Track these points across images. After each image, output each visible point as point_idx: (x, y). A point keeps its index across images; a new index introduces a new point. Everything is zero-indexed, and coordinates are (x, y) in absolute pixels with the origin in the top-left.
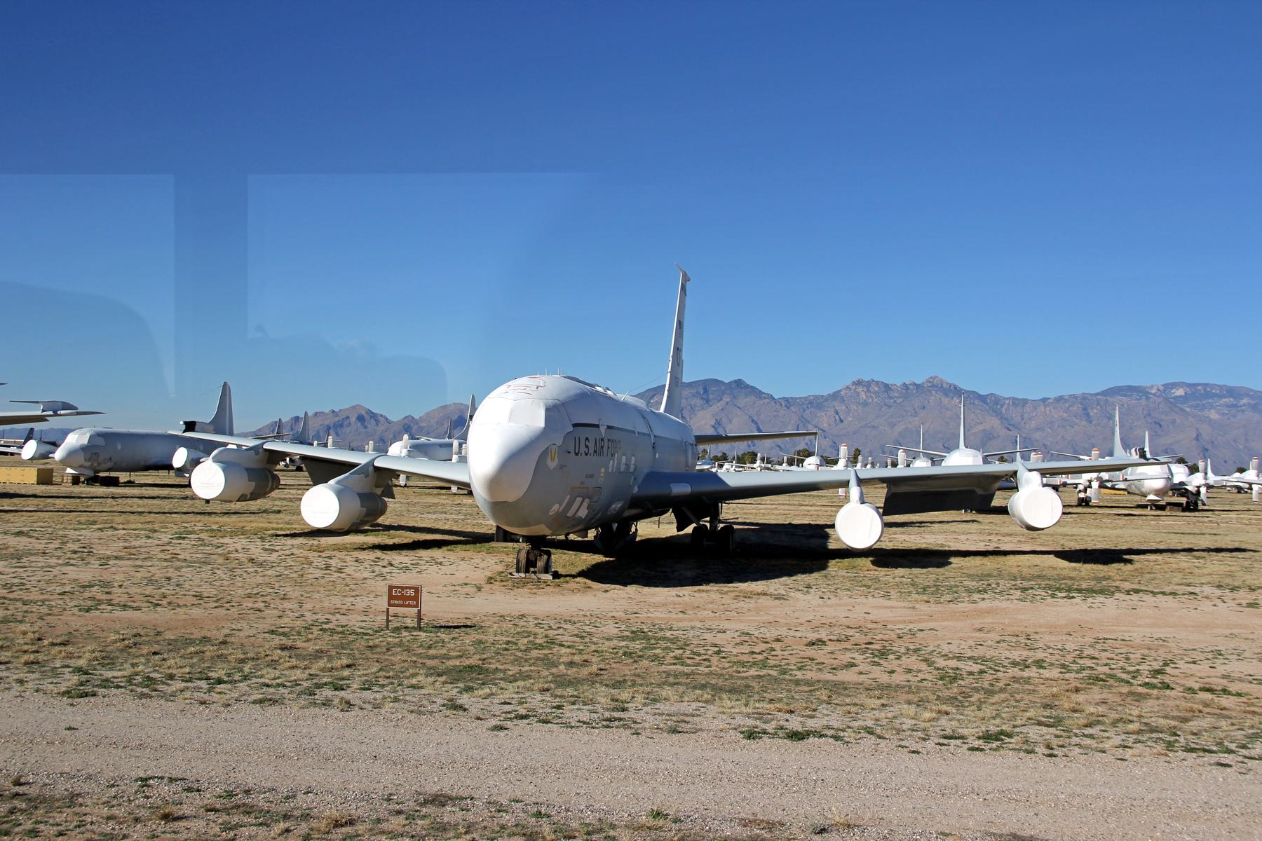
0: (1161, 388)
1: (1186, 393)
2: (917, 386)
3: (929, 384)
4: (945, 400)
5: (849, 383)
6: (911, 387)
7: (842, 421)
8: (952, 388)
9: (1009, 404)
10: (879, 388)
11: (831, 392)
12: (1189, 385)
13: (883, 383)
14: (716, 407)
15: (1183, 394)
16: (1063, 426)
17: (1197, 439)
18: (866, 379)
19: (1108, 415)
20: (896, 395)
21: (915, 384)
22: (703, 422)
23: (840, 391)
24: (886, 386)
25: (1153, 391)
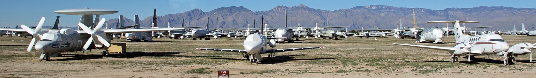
0: (369, 7)
3: (300, 7)
4: (304, 11)
5: (275, 7)
6: (295, 8)
7: (273, 18)
11: (270, 10)
12: (377, 6)
14: (234, 15)
15: (375, 8)
16: (339, 19)
17: (376, 22)
18: (281, 5)
19: (352, 15)
21: (296, 7)
22: (229, 20)
23: (273, 9)
24: (287, 7)
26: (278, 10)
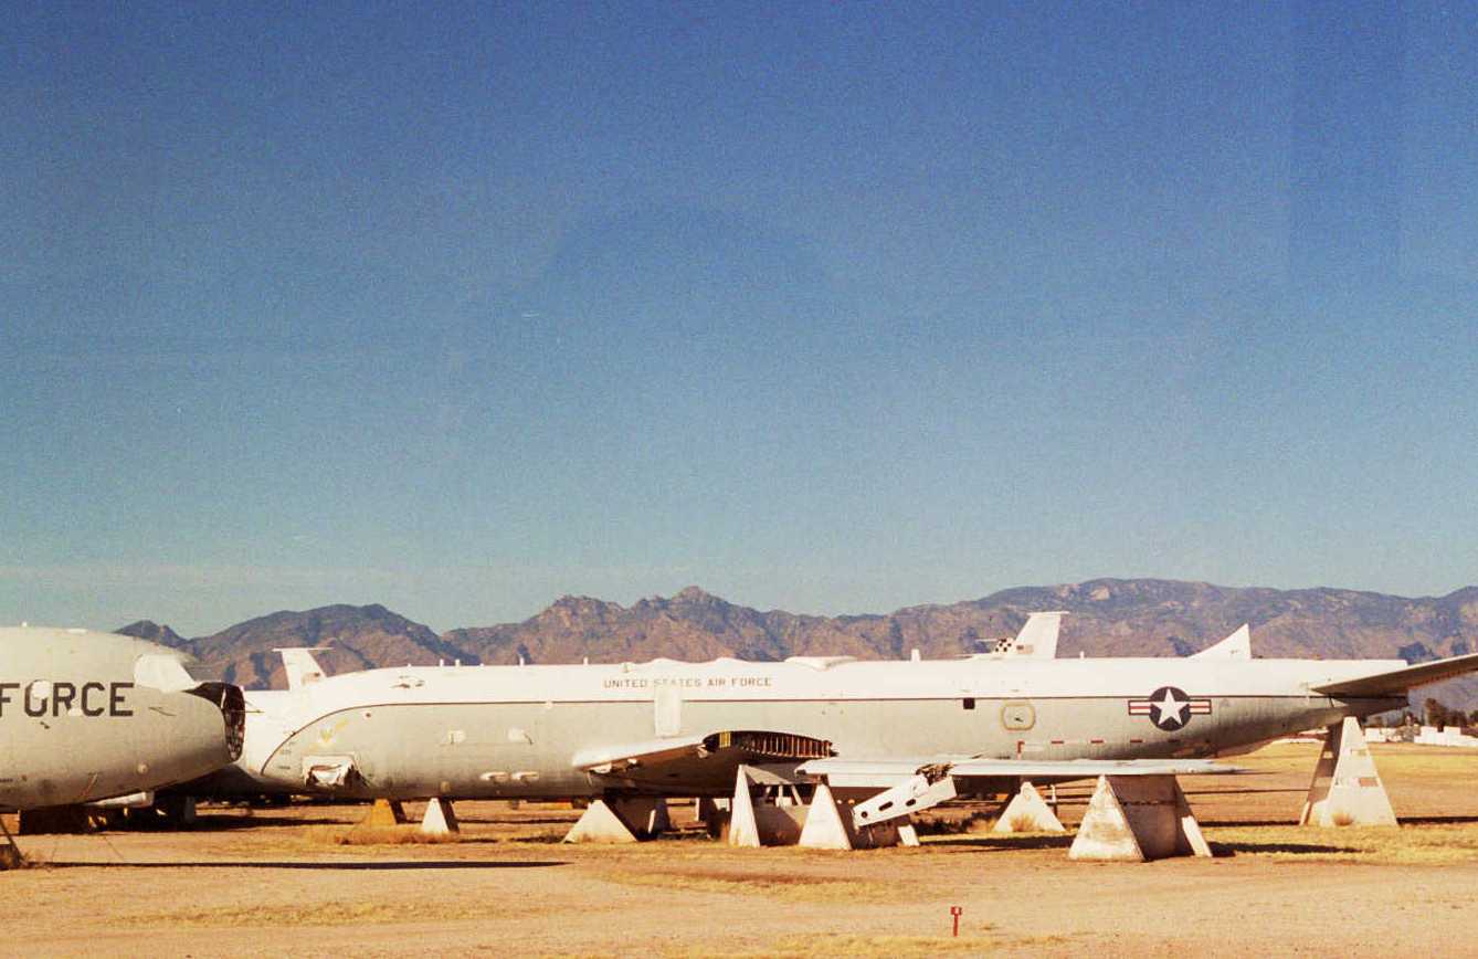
0: (1076, 588)
1: (1111, 594)
2: (663, 604)
5: (550, 602)
8: (713, 604)
9: (795, 626)
10: (591, 608)
12: (1121, 583)
13: (597, 601)
20: (614, 619)
23: (538, 616)
25: (1064, 594)
26: (560, 620)
